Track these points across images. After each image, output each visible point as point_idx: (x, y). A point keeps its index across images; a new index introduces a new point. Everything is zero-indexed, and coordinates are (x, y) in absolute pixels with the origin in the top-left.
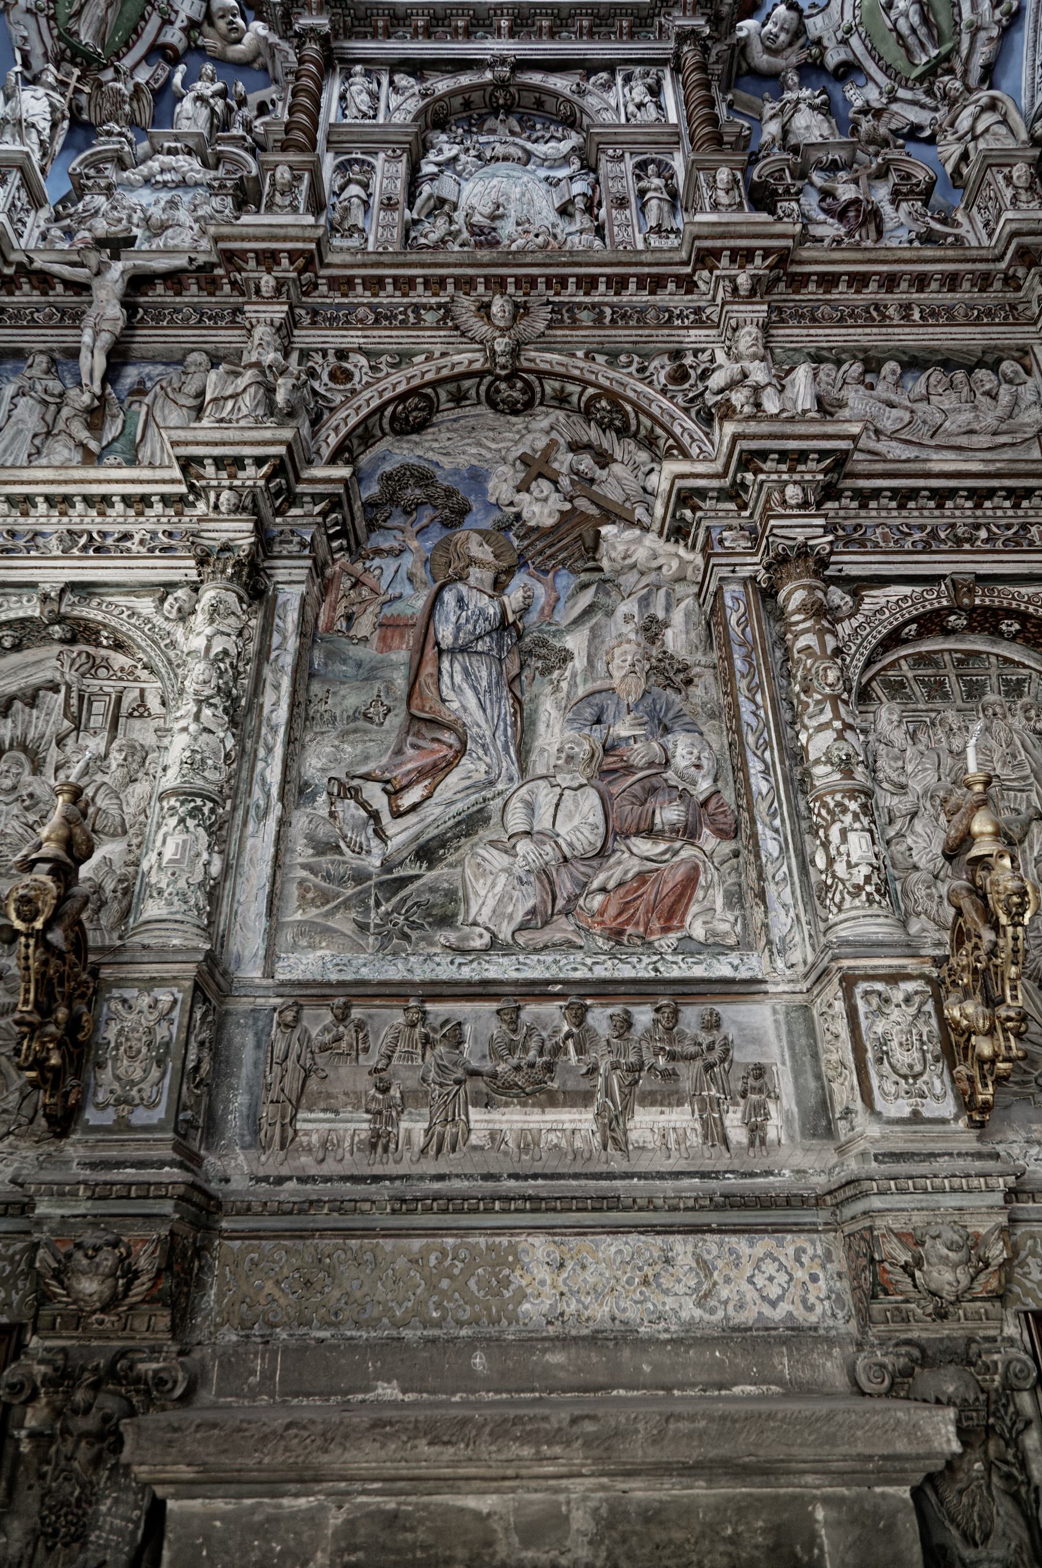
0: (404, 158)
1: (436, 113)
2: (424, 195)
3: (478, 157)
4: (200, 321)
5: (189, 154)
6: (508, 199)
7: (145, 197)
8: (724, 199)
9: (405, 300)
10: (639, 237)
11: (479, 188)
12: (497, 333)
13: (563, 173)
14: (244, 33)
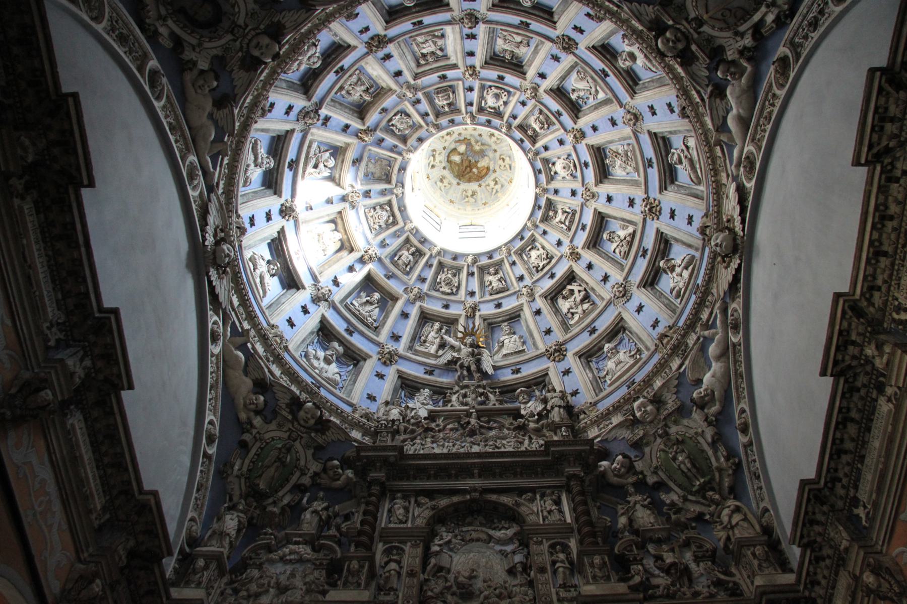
2: (432, 564)
3: (462, 540)
5: (305, 544)
6: (479, 566)
7: (279, 568)
8: (600, 574)
11: (462, 559)
13: (509, 548)
14: (341, 475)
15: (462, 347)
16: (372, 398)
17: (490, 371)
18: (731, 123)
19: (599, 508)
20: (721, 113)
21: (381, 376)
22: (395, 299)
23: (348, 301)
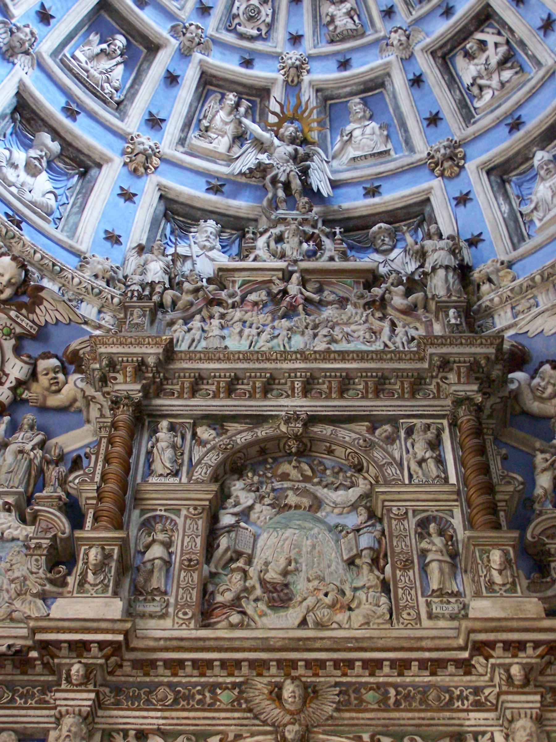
0: (204, 515)
1: (235, 462)
4: (12, 700)
6: (299, 553)
8: (498, 579)
9: (203, 679)
10: (422, 600)
12: (288, 718)
15: (276, 142)
16: (113, 238)
17: (326, 190)
19: (505, 458)
21: (127, 196)
22: (153, 48)
23: (67, 51)
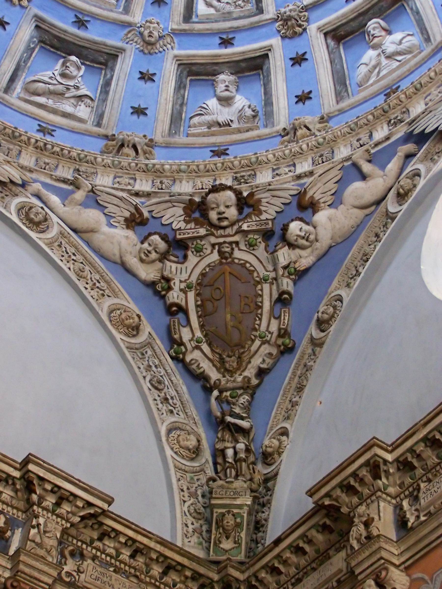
18: (91, 216)
20: (111, 208)
